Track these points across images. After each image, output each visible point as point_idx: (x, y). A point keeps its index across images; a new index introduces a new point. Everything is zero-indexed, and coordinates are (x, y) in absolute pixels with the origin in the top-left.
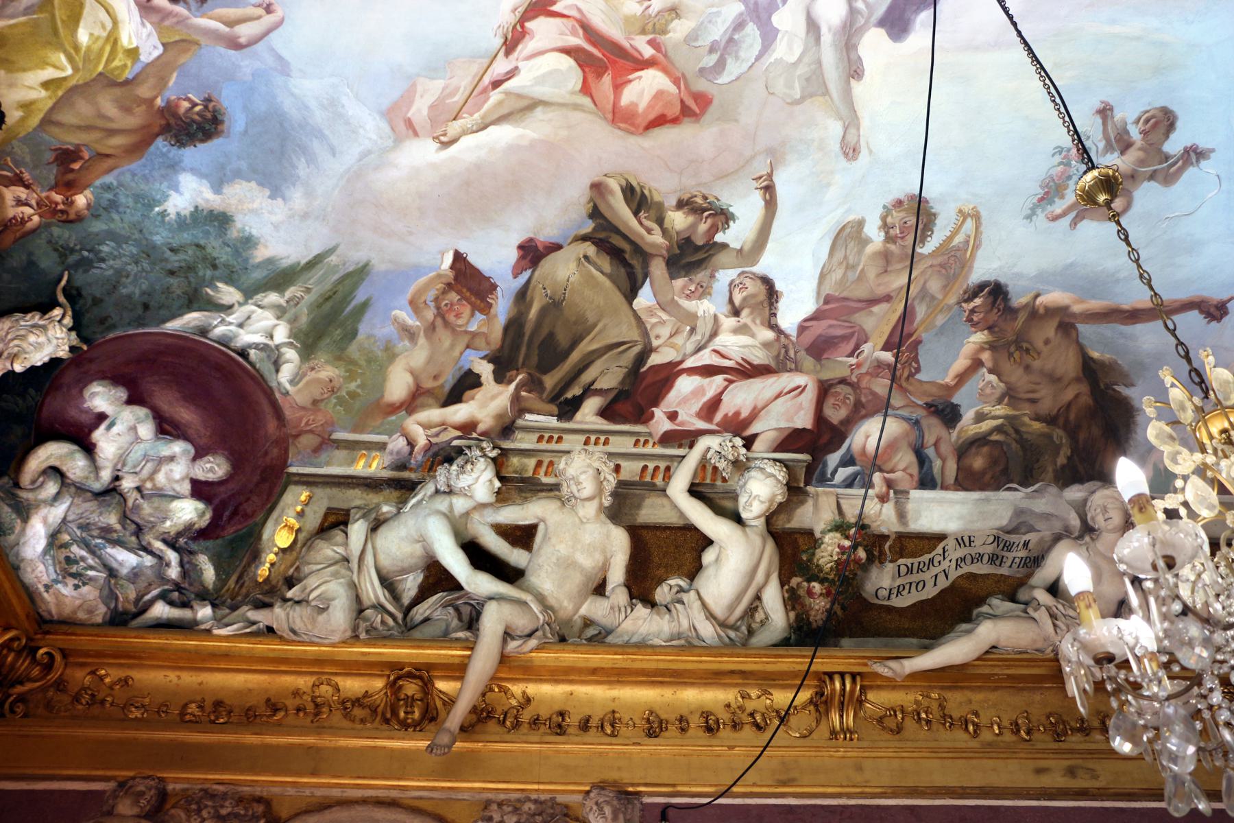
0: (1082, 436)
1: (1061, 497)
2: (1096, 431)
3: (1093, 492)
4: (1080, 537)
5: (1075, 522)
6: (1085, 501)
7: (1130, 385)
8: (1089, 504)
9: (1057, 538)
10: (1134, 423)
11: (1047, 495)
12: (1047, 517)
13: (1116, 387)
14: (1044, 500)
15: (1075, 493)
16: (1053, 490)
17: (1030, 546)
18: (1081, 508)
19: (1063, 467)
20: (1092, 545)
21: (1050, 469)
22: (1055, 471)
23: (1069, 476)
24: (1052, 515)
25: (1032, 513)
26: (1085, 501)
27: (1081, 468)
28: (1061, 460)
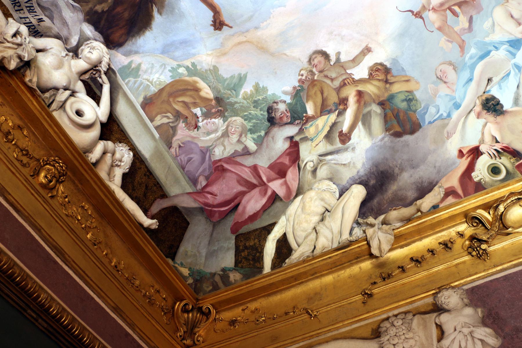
0: (119, 9)
1: (81, 24)
2: (126, 15)
3: (96, 40)
4: (69, 51)
5: (74, 41)
6: (88, 39)
7: (160, 13)
8: (88, 42)
9: (58, 37)
10: (144, 32)
11: (76, 14)
12: (65, 23)
13: (154, 5)
14: (72, 14)
15: (88, 30)
16: (81, 16)
17: (42, 24)
18: (83, 40)
19: (96, 12)
20: (70, 57)
21: (90, 5)
22: (91, 9)
23: (93, 19)
24: (68, 26)
25: (60, 12)
26: (88, 39)
27: (103, 22)
28: (99, 8)
